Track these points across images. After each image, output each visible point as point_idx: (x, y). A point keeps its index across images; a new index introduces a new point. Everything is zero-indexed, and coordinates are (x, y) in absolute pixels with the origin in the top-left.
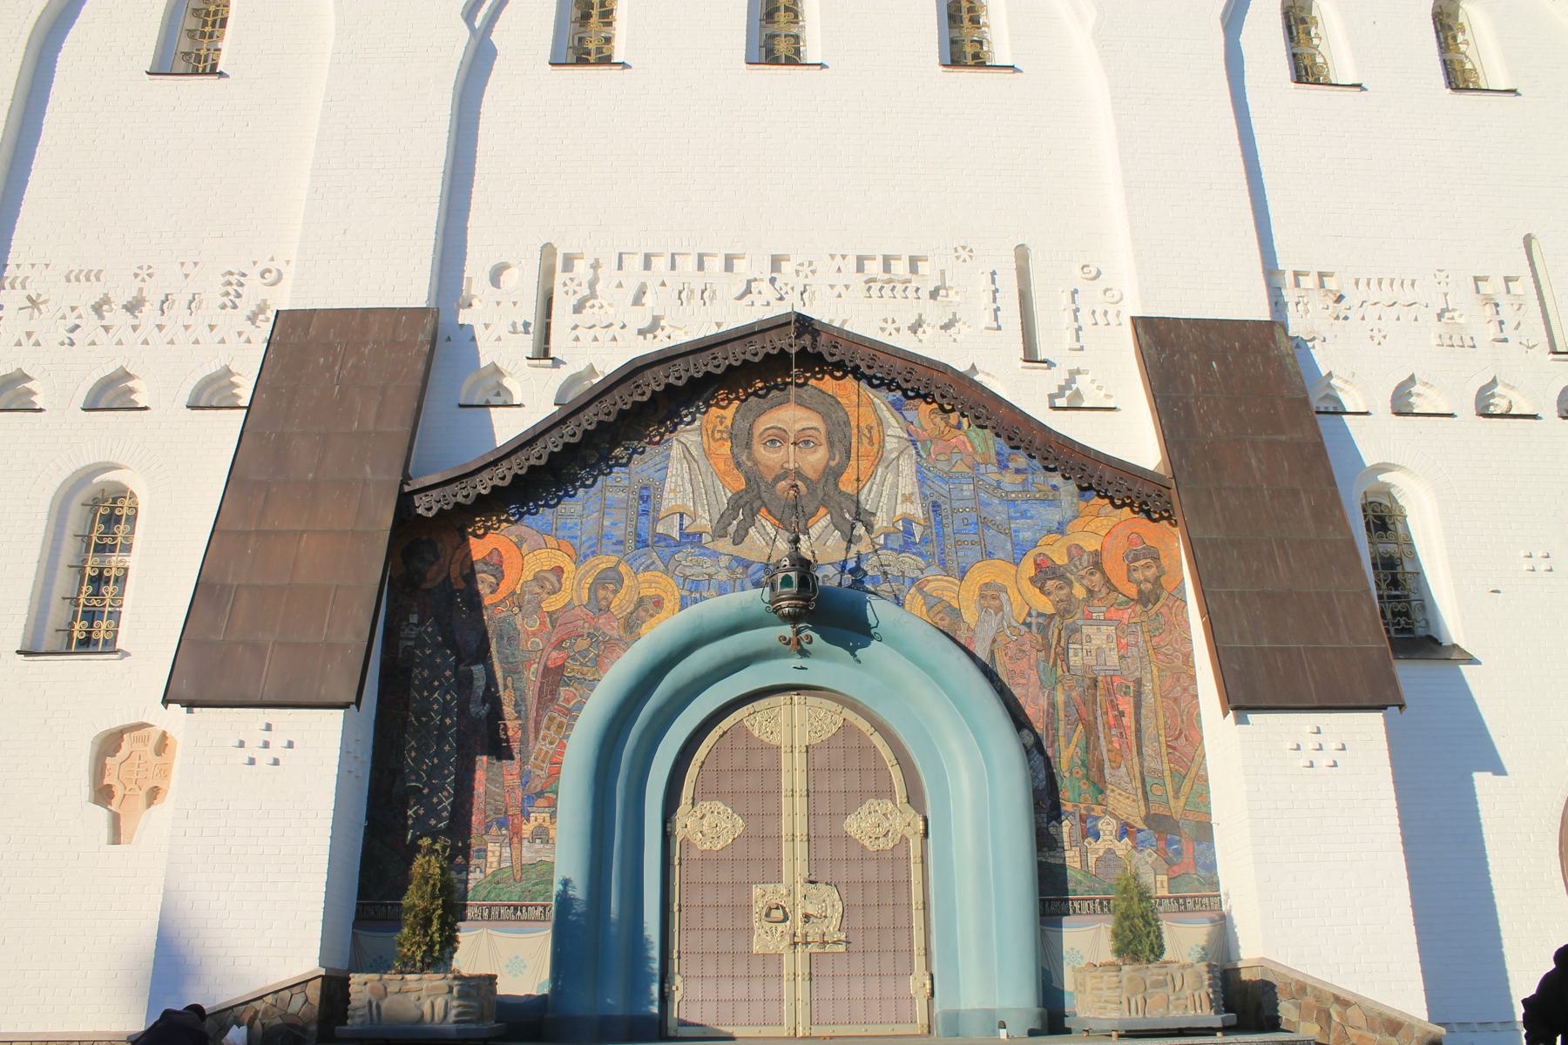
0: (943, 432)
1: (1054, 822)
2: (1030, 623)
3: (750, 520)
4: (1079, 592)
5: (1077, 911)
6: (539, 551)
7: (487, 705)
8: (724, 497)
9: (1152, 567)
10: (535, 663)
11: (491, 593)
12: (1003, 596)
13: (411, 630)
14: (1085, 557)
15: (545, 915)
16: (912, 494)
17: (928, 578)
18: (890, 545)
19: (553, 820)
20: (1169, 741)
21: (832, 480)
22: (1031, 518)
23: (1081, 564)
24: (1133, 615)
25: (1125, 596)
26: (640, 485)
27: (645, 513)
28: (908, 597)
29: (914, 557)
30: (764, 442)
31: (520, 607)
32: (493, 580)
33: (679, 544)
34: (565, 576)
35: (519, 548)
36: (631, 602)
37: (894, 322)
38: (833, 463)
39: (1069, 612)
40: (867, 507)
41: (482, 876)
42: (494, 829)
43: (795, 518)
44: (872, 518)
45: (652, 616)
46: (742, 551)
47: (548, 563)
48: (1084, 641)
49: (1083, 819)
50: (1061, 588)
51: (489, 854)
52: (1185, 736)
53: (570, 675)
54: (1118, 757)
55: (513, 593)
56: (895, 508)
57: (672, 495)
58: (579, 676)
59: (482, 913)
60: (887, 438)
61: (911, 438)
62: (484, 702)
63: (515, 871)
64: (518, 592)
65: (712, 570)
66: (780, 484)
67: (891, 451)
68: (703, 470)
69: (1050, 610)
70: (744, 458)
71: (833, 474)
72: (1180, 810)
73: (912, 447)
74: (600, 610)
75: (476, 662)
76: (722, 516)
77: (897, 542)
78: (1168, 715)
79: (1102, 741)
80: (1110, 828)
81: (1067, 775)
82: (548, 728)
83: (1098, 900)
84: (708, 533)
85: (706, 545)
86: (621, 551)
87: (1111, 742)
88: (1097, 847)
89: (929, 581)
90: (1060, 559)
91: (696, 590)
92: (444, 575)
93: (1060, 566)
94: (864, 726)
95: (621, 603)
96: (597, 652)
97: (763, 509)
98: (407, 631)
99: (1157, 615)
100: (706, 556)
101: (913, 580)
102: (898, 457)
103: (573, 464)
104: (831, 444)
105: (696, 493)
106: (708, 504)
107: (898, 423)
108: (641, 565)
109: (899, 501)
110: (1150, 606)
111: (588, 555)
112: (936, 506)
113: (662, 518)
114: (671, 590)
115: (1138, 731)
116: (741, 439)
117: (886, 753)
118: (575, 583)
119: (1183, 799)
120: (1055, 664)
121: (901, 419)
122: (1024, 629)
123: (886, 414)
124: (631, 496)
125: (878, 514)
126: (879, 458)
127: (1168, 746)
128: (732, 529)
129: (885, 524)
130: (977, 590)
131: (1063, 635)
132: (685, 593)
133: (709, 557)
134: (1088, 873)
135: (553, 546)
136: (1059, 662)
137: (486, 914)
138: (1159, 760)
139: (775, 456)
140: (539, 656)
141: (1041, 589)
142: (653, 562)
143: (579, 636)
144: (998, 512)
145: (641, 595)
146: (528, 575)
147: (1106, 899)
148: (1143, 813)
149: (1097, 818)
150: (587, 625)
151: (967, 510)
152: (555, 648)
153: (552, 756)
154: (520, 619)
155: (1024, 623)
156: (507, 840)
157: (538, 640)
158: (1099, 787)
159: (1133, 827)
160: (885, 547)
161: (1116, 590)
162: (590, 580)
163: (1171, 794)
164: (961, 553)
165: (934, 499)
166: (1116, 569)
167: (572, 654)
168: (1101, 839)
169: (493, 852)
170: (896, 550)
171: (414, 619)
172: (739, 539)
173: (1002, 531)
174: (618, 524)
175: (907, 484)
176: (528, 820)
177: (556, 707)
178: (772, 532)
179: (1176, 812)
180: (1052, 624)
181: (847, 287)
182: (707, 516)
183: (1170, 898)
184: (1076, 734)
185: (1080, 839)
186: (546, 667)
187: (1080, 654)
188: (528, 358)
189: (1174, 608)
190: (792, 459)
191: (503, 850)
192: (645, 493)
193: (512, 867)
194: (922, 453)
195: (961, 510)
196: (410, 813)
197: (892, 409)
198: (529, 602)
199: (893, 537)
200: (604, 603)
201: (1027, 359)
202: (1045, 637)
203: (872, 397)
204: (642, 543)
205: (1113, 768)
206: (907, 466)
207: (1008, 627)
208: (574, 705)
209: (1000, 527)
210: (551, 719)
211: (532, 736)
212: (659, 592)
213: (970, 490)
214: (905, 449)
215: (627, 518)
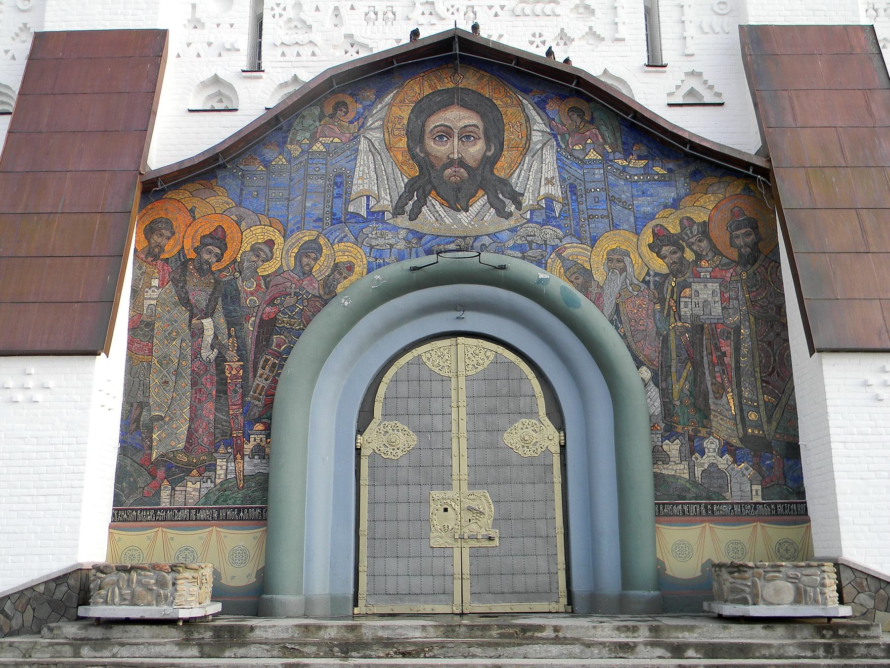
0: (579, 126)
1: (667, 441)
2: (649, 281)
3: (422, 202)
4: (689, 255)
5: (686, 512)
6: (254, 227)
7: (215, 350)
8: (402, 182)
9: (751, 235)
10: (253, 316)
11: (217, 261)
12: (627, 260)
13: (153, 291)
14: (695, 227)
15: (262, 516)
16: (553, 177)
17: (566, 246)
18: (535, 219)
19: (269, 440)
20: (764, 377)
21: (488, 166)
22: (651, 195)
23: (691, 233)
24: (734, 274)
25: (728, 258)
26: (335, 174)
27: (339, 196)
28: (549, 261)
29: (555, 229)
30: (434, 137)
31: (240, 273)
32: (219, 251)
33: (366, 221)
34: (275, 247)
35: (239, 226)
36: (329, 268)
37: (540, 35)
38: (489, 154)
39: (681, 272)
40: (517, 189)
41: (212, 485)
42: (222, 449)
44: (521, 198)
45: (345, 278)
46: (416, 225)
47: (262, 237)
48: (693, 295)
49: (691, 439)
50: (675, 253)
51: (218, 468)
52: (777, 373)
53: (281, 325)
54: (720, 391)
55: (235, 261)
56: (539, 190)
57: (360, 182)
58: (288, 326)
59: (213, 514)
60: (533, 132)
61: (553, 132)
62: (212, 347)
63: (238, 481)
64: (239, 260)
65: (392, 241)
66: (446, 171)
67: (536, 143)
68: (385, 160)
69: (665, 270)
70: (418, 150)
71: (489, 162)
72: (772, 433)
73: (553, 140)
74: (304, 274)
75: (206, 317)
76: (400, 198)
77: (540, 217)
78: (762, 355)
79: (708, 377)
80: (713, 446)
81: (678, 403)
82: (263, 368)
83: (703, 505)
84: (389, 212)
85: (387, 221)
86: (320, 227)
87: (715, 377)
88: (702, 461)
89: (566, 248)
90: (674, 228)
91: (380, 256)
92: (179, 247)
93: (673, 235)
95: (321, 268)
96: (301, 307)
97: (433, 192)
98: (150, 292)
99: (755, 274)
100: (387, 230)
101: (554, 247)
102: (542, 148)
103: (281, 157)
104: (488, 140)
105: (380, 179)
106: (389, 188)
107: (543, 120)
108: (336, 238)
109: (543, 184)
110: (749, 266)
111: (294, 230)
112: (573, 188)
113: (353, 200)
114: (360, 257)
115: (738, 368)
116: (416, 136)
118: (284, 252)
119: (774, 424)
120: (669, 314)
121: (544, 116)
122: (643, 286)
123: (532, 113)
124: (328, 182)
125: (526, 194)
126: (526, 149)
127: (763, 381)
128: (408, 208)
129: (531, 202)
130: (605, 254)
131: (675, 291)
132: (371, 260)
133: (390, 231)
134: (695, 482)
135: (266, 224)
136: (672, 312)
137: (215, 515)
138: (755, 392)
139: (443, 148)
140: (256, 311)
141: (658, 255)
142: (346, 235)
143: (287, 295)
144: (623, 191)
145: (336, 262)
146: (246, 247)
147: (710, 504)
148: (741, 436)
149: (704, 438)
150: (293, 286)
151: (598, 190)
152: (268, 305)
153: (268, 390)
154: (240, 282)
155: (644, 281)
156: (232, 457)
157: (255, 298)
158: (704, 413)
159: (732, 446)
160: (530, 221)
161: (721, 254)
162: (296, 250)
163: (764, 419)
164: (592, 226)
165: (571, 181)
167: (282, 309)
168: (706, 456)
169: (221, 466)
170: (539, 224)
171: (155, 283)
172: (413, 216)
173: (627, 207)
174: (315, 206)
175: (550, 168)
176: (249, 441)
177: (270, 351)
179: (769, 434)
180: (667, 281)
181: (502, 7)
182: (388, 198)
183: (764, 503)
184: (686, 371)
185: (688, 454)
186: (261, 319)
187: (690, 306)
188: (244, 71)
189: (770, 269)
190: (456, 150)
191: (229, 465)
192: (339, 180)
193: (236, 477)
194: (561, 143)
195: (593, 190)
196: (154, 436)
197: (538, 109)
198: (247, 269)
199: (537, 213)
200: (307, 268)
201: (651, 64)
202: (661, 292)
203: (521, 98)
204: (336, 220)
205: (716, 398)
206: (549, 156)
207: (630, 285)
208: (284, 349)
209: (625, 204)
210: (267, 361)
211: (251, 375)
212: (351, 259)
213: (600, 174)
214: (547, 141)
215: (324, 199)
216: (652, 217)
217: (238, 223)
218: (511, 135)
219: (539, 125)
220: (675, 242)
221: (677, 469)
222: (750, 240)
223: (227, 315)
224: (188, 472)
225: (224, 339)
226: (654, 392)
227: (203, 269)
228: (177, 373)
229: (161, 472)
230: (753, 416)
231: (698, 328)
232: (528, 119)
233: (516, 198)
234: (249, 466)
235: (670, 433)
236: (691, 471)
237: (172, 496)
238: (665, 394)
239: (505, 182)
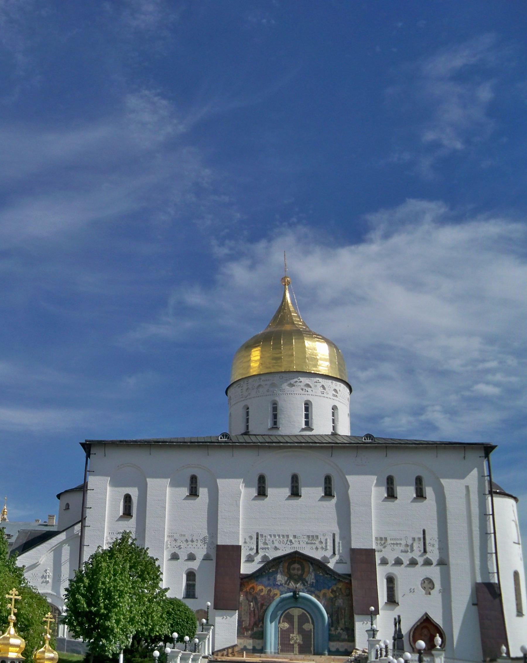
3: (290, 582)
4: (337, 594)
27: (274, 581)
33: (280, 585)
46: (289, 587)
54: (341, 619)
62: (253, 608)
75: (251, 602)
90: (335, 589)
94: (305, 612)
112: (317, 581)
116: (289, 569)
117: (309, 617)
123: (310, 565)
126: (309, 572)
146: (258, 589)
158: (338, 623)
162: (267, 591)
171: (242, 596)
172: (288, 585)
175: (313, 577)
178: (293, 585)
204: (274, 585)
206: (313, 574)
216: (331, 587)
217: (257, 585)
218: (306, 570)
221: (333, 633)
222: (349, 591)
223: (255, 602)
224: (249, 630)
225: (255, 607)
226: (330, 619)
227: (250, 593)
228: (247, 613)
229: (245, 629)
230: (346, 624)
232: (310, 567)
233: (307, 582)
234: (260, 629)
235: (332, 626)
236: (336, 633)
237: (247, 634)
238: (332, 620)
239: (305, 579)
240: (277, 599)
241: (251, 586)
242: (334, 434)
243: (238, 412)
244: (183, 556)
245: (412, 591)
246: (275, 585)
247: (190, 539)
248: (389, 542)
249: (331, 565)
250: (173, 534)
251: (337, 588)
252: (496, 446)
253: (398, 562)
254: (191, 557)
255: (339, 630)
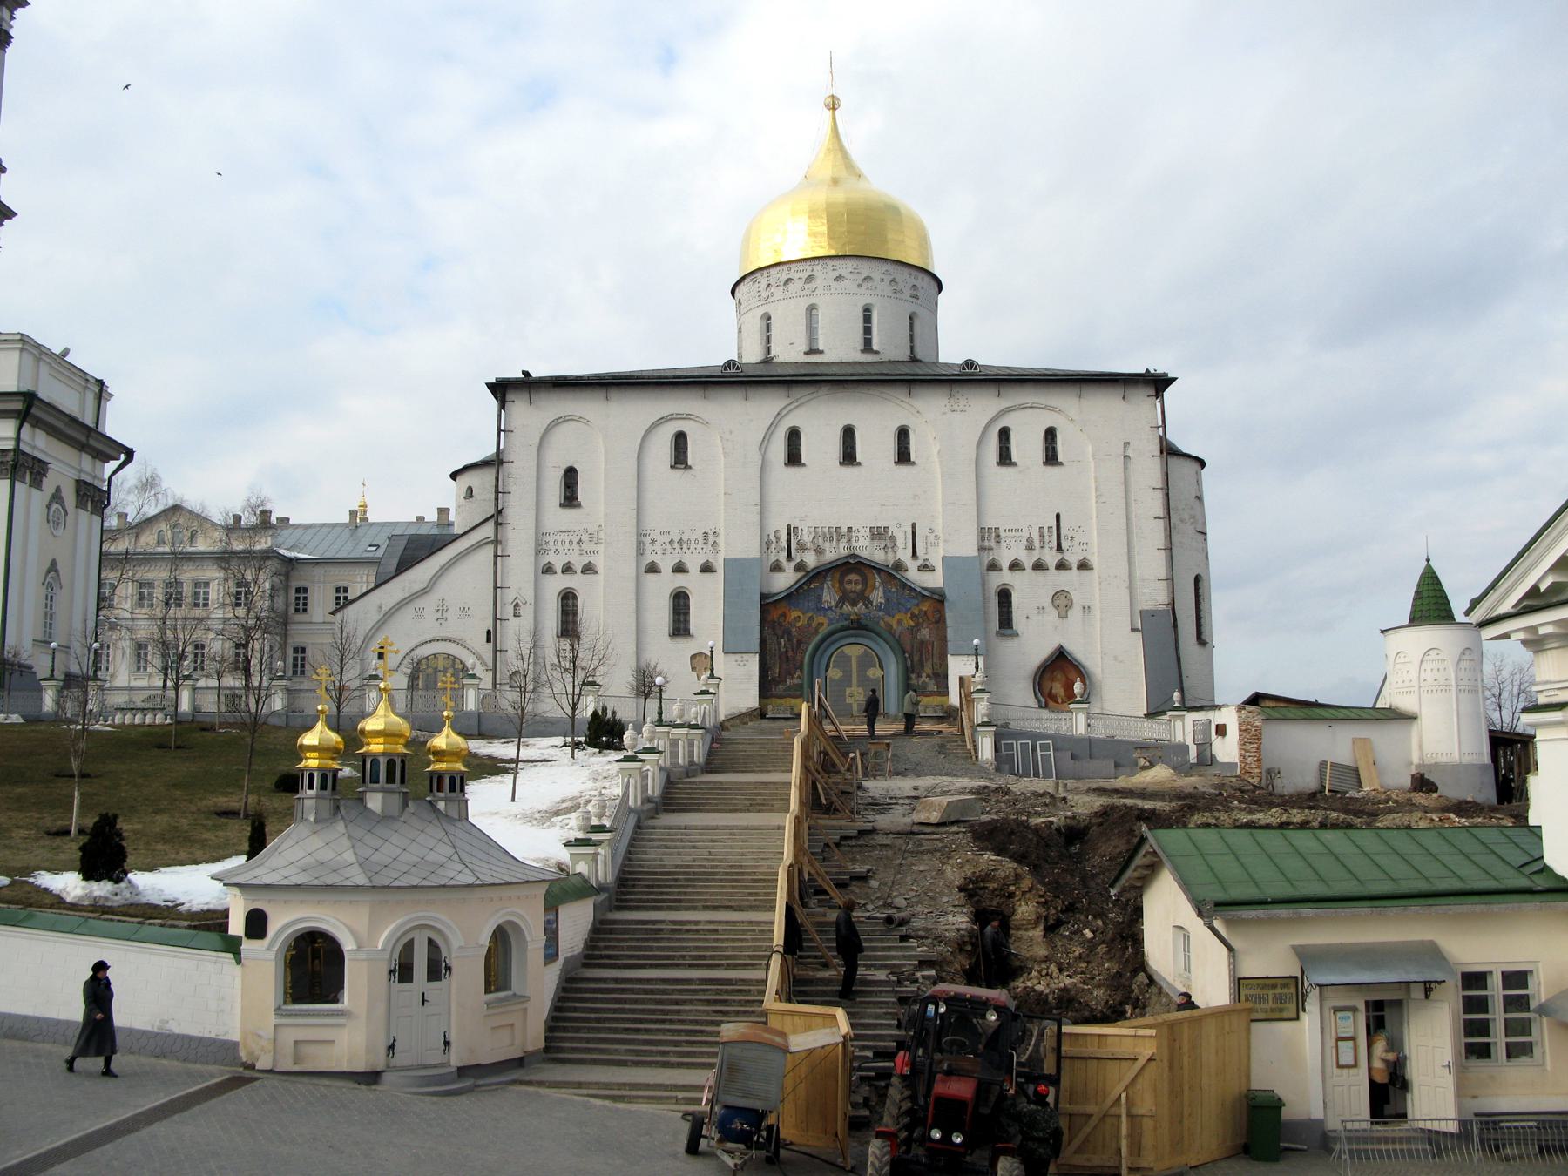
4: (921, 620)
43: (854, 604)
54: (927, 660)
71: (863, 591)
90: (916, 612)
95: (814, 624)
112: (887, 600)
116: (841, 582)
126: (874, 587)
144: (903, 601)
158: (923, 666)
166: (930, 614)
172: (842, 606)
175: (881, 594)
206: (881, 589)
219: (878, 579)
220: (916, 616)
227: (780, 624)
231: (922, 642)
233: (871, 603)
235: (913, 672)
238: (912, 661)
240: (823, 631)
241: (780, 612)
242: (914, 360)
243: (754, 323)
244: (666, 565)
245: (1041, 610)
246: (820, 609)
247: (676, 539)
248: (1002, 534)
249: (913, 575)
250: (649, 532)
251: (920, 611)
252: (1174, 379)
253: (1015, 566)
254: (680, 569)
255: (924, 678)
